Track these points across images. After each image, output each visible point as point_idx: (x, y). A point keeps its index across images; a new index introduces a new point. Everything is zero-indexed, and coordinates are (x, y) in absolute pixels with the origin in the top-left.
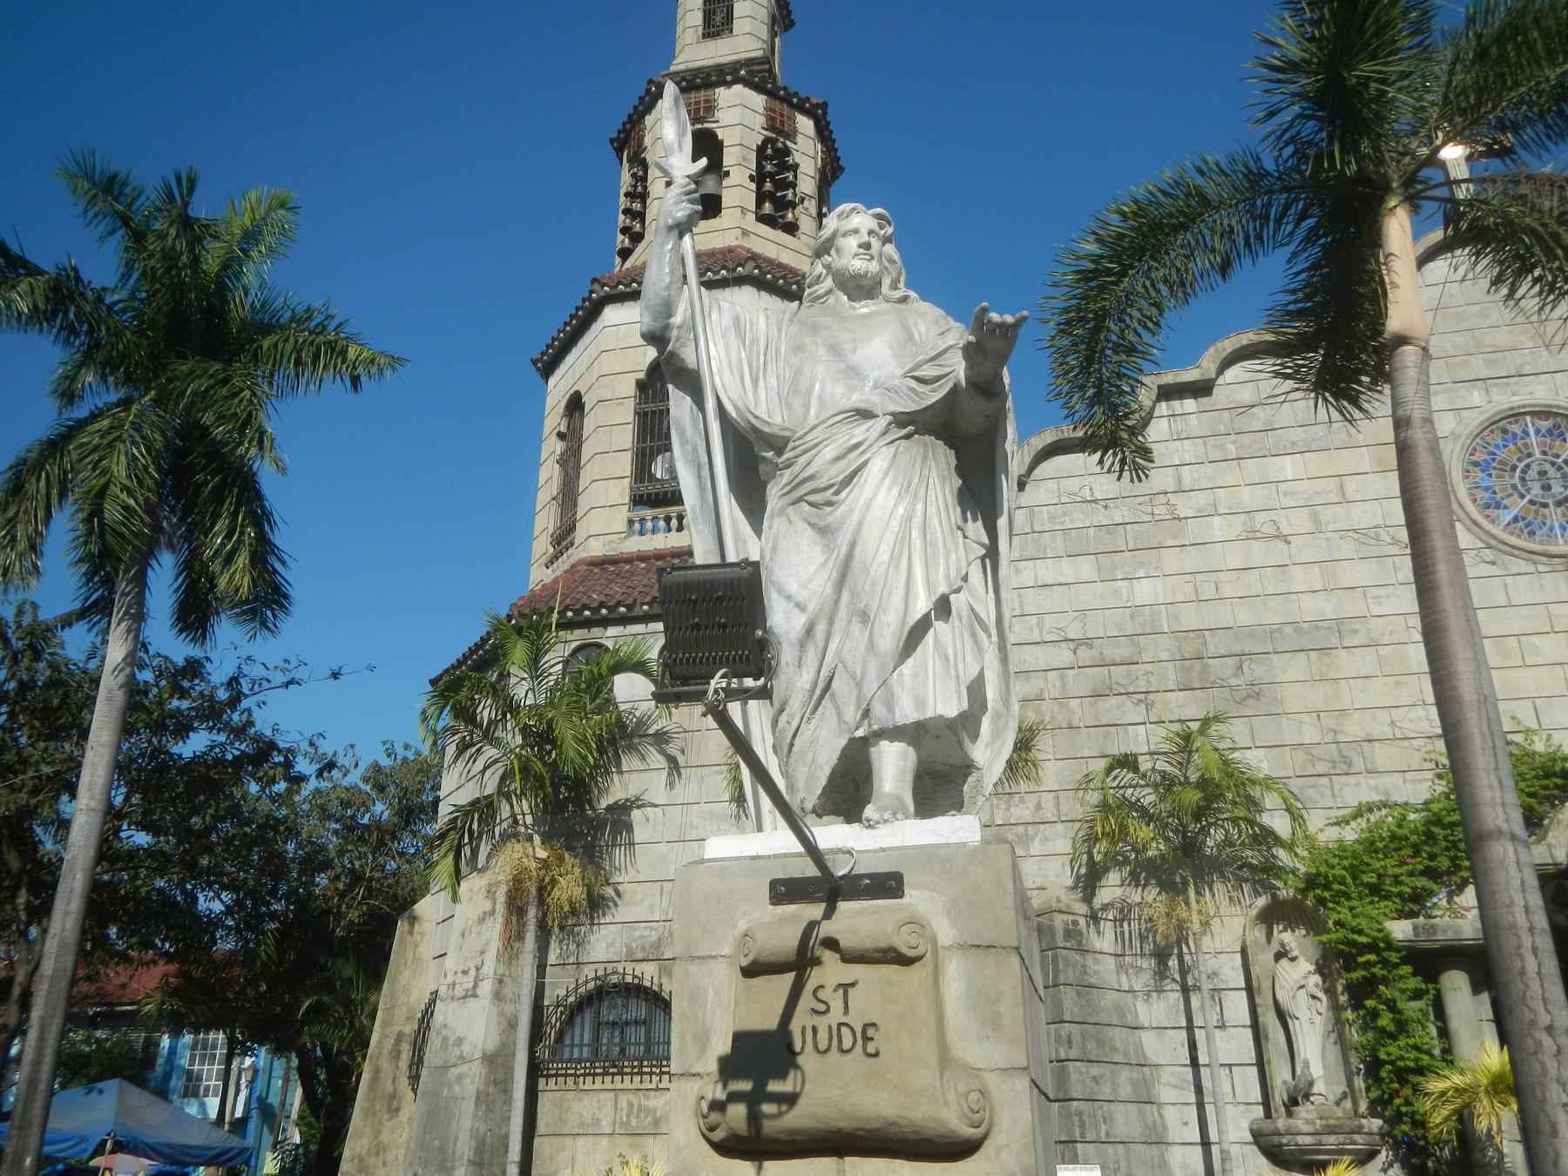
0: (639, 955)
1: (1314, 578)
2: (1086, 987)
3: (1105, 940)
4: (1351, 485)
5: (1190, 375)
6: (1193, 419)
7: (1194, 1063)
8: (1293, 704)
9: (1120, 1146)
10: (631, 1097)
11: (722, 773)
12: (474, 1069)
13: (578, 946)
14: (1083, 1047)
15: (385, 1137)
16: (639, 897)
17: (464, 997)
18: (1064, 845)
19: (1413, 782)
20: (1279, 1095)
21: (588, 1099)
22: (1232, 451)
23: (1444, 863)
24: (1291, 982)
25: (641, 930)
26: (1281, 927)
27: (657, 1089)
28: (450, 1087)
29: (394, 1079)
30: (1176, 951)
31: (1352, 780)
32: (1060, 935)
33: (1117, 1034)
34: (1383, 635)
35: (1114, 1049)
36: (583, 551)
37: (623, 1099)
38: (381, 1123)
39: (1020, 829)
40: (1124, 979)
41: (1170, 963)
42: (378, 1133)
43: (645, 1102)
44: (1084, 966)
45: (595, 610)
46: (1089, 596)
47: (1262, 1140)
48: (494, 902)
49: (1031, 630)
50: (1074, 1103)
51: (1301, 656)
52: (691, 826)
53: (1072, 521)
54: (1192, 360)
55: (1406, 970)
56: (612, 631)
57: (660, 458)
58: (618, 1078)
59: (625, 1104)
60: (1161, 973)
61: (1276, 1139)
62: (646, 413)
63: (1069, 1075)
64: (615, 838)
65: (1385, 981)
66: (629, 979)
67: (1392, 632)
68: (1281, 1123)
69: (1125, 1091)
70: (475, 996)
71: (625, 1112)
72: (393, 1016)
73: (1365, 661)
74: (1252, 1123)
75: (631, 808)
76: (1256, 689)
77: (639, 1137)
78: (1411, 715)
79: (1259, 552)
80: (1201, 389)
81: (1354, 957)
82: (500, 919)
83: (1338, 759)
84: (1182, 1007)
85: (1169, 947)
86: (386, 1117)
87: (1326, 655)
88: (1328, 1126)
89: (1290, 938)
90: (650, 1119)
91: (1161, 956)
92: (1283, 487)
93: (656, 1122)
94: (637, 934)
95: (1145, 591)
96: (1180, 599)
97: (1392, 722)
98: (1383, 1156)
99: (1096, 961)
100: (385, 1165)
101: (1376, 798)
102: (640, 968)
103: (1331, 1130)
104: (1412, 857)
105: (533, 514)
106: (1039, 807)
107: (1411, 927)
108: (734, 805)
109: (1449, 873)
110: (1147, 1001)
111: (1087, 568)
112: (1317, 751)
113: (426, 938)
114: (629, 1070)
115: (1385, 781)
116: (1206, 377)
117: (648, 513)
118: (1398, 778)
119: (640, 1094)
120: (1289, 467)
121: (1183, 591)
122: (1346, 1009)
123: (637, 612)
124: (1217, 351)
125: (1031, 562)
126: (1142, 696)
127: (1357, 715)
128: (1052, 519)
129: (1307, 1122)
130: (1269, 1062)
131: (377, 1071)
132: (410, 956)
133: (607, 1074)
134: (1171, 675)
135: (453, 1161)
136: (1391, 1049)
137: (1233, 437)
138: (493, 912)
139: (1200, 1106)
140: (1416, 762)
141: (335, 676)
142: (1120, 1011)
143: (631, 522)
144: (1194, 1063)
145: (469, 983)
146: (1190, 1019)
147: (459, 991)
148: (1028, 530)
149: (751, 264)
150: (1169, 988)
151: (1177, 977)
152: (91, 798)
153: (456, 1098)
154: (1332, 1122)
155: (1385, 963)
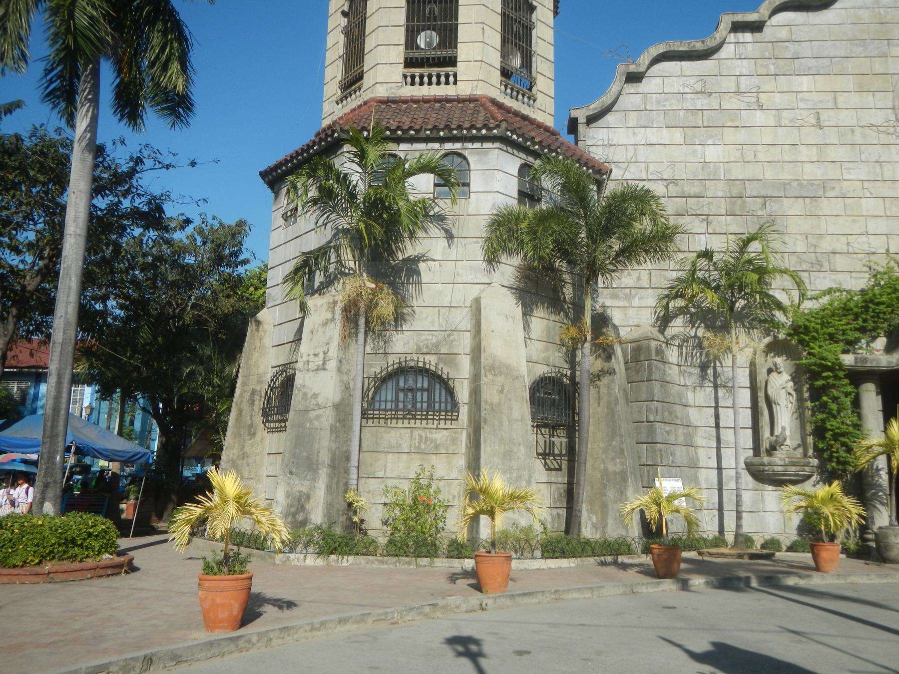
0: (425, 350)
1: (812, 153)
2: (665, 382)
3: (673, 355)
4: (841, 98)
5: (752, 17)
6: (750, 46)
7: (717, 426)
8: (792, 229)
9: (678, 468)
10: (421, 432)
12: (327, 412)
13: (385, 343)
14: (663, 415)
15: (247, 449)
16: (424, 315)
17: (317, 370)
18: (652, 301)
19: (856, 278)
20: (765, 445)
21: (393, 432)
22: (772, 69)
23: (870, 325)
24: (778, 385)
25: (425, 336)
26: (772, 355)
27: (437, 428)
28: (311, 422)
29: (251, 416)
30: (712, 365)
31: (821, 275)
32: (653, 352)
33: (678, 408)
34: (849, 192)
35: (676, 417)
36: (372, 93)
37: (416, 433)
38: (244, 441)
39: (627, 291)
40: (682, 378)
41: (709, 371)
42: (243, 447)
43: (428, 435)
44: (664, 371)
45: (393, 131)
46: (677, 153)
47: (752, 468)
48: (333, 313)
49: (641, 171)
50: (658, 445)
51: (801, 200)
52: (458, 274)
53: (670, 105)
54: (754, 8)
55: (846, 381)
56: (403, 146)
57: (423, 34)
58: (412, 421)
59: (417, 436)
60: (703, 376)
61: (761, 468)
63: (655, 430)
64: (408, 279)
65: (834, 386)
66: (421, 364)
67: (854, 190)
68: (766, 459)
69: (681, 439)
70: (324, 369)
71: (417, 440)
73: (837, 206)
74: (746, 459)
75: (418, 261)
76: (773, 218)
77: (427, 455)
78: (859, 240)
79: (782, 135)
80: (756, 27)
81: (819, 373)
82: (339, 324)
83: (815, 262)
84: (713, 396)
85: (709, 361)
86: (248, 438)
87: (815, 201)
88: (792, 462)
89: (779, 360)
90: (433, 445)
91: (703, 367)
92: (800, 95)
93: (437, 447)
94: (424, 337)
95: (712, 153)
96: (732, 160)
97: (848, 243)
98: (814, 478)
99: (670, 368)
100: (248, 465)
101: (834, 286)
102: (428, 358)
103: (794, 464)
104: (854, 320)
105: (324, 67)
106: (639, 278)
107: (853, 359)
108: (485, 264)
109: (870, 331)
110: (694, 391)
111: (677, 136)
112: (804, 257)
114: (419, 417)
115: (840, 277)
116: (762, 19)
117: (417, 71)
118: (847, 275)
119: (426, 430)
120: (805, 83)
121: (735, 155)
122: (807, 401)
123: (422, 135)
125: (644, 129)
126: (705, 217)
127: (828, 238)
128: (658, 102)
129: (781, 459)
130: (762, 427)
131: (240, 412)
132: (258, 344)
133: (406, 418)
134: (723, 206)
135: (317, 465)
136: (835, 424)
137: (773, 61)
138: (333, 319)
139: (718, 449)
140: (859, 266)
141: (193, 164)
142: (680, 396)
143: (405, 76)
144: (717, 426)
146: (717, 402)
147: (312, 366)
148: (642, 108)
150: (706, 385)
151: (712, 379)
153: (317, 429)
154: (794, 460)
155: (836, 377)
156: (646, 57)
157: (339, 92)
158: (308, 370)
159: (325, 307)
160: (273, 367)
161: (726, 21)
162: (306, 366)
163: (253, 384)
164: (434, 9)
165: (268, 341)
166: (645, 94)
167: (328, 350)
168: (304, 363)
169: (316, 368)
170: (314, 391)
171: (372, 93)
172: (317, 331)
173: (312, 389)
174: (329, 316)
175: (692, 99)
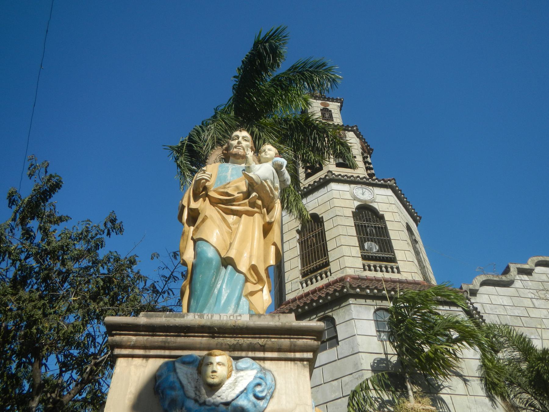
5: (526, 266)
11: (474, 381)
36: (343, 272)
53: (499, 311)
54: (526, 263)
80: (529, 272)
116: (532, 268)
117: (372, 263)
124: (532, 260)
143: (364, 266)
149: (393, 181)
156: (477, 281)
157: (300, 276)
161: (513, 268)
164: (372, 230)
166: (482, 304)
171: (343, 272)
175: (511, 309)
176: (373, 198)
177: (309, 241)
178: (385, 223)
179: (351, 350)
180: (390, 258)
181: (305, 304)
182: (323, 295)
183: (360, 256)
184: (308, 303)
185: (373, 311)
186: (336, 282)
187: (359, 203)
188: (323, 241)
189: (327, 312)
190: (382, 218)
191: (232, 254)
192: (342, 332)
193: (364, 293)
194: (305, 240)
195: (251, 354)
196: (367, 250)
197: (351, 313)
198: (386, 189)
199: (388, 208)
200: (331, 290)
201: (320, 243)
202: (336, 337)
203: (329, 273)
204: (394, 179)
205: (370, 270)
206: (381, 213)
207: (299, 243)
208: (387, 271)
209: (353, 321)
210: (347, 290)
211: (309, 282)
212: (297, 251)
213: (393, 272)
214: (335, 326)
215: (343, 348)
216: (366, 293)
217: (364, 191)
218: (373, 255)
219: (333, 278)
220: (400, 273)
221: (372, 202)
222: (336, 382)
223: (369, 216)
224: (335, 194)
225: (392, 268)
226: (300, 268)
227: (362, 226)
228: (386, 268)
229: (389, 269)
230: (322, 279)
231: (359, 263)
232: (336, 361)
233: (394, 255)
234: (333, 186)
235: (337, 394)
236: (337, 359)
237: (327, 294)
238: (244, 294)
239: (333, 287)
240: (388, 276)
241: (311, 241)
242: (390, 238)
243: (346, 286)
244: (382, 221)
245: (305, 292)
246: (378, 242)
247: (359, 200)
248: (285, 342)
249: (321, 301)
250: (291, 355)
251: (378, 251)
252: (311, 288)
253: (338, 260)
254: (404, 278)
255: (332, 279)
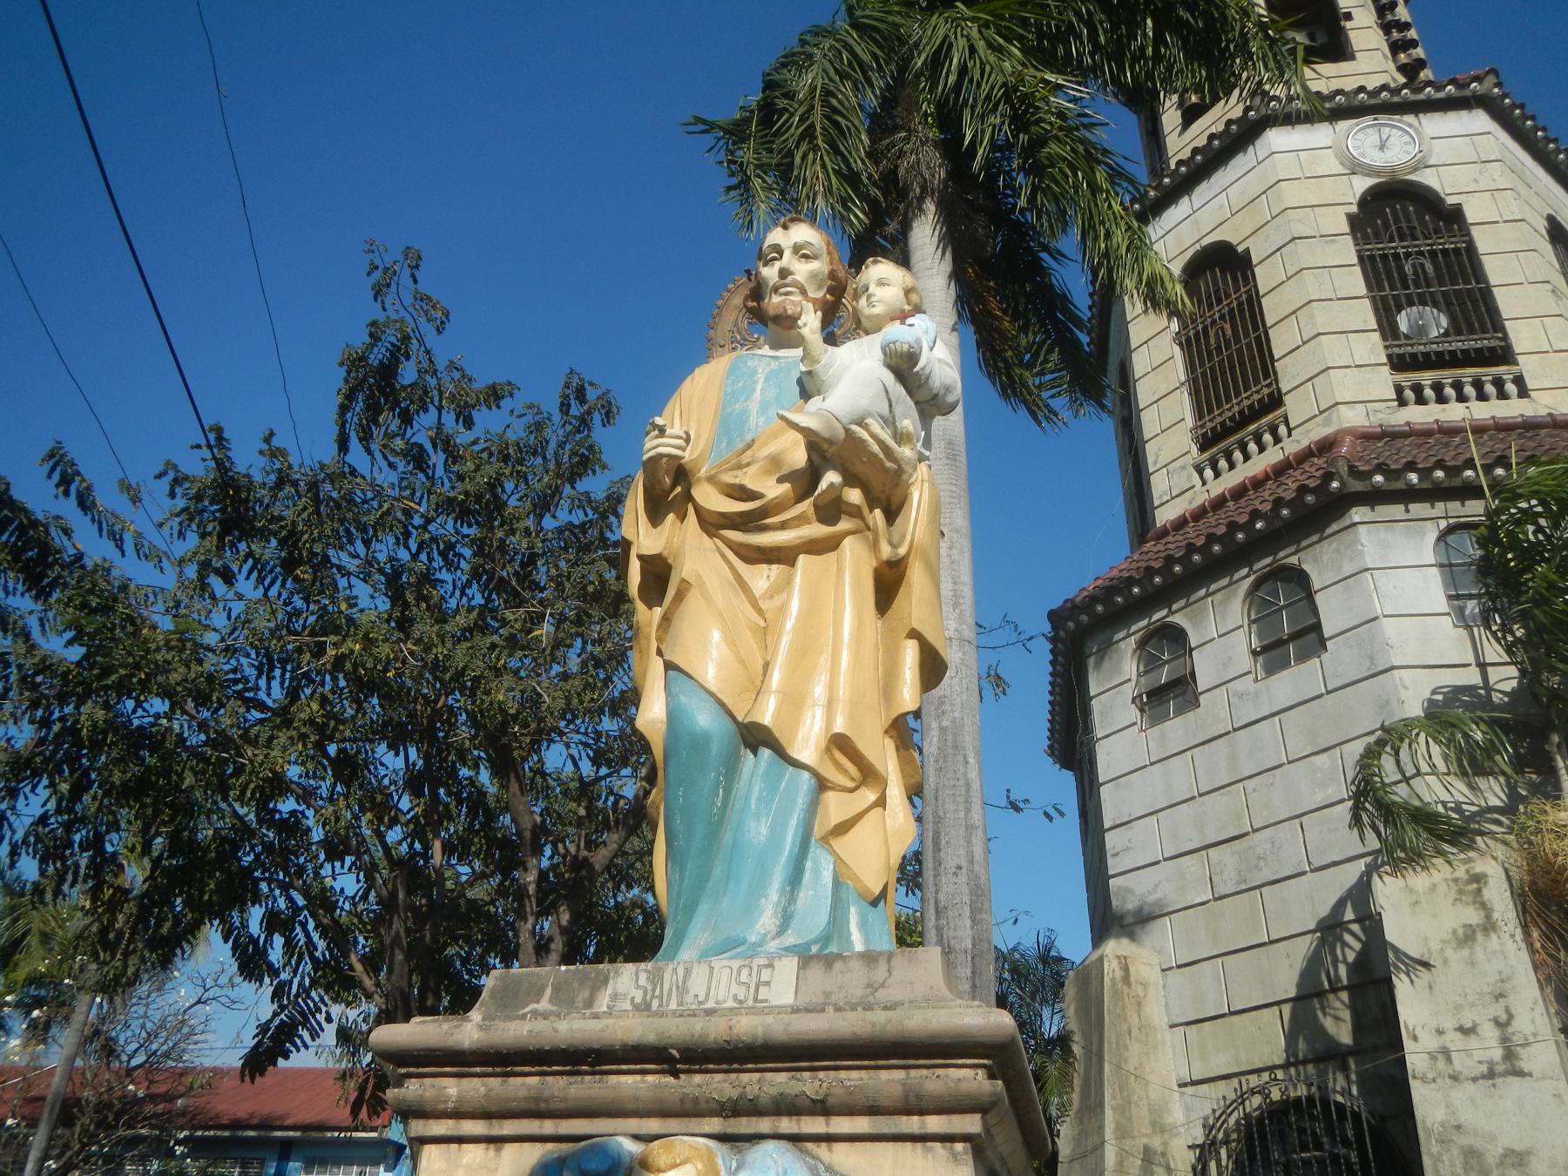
17: (1491, 1075)
36: (1327, 423)
48: (1484, 907)
62: (1372, 258)
70: (1520, 1073)
72: (1130, 1119)
113: (1152, 991)
117: (1426, 378)
138: (1489, 926)
143: (1399, 390)
145: (1488, 1047)
149: (1491, 79)
152: (961, 620)
157: (1194, 449)
158: (1455, 1078)
159: (1445, 894)
160: (1182, 1085)
162: (1441, 1064)
163: (1144, 1137)
164: (1422, 266)
165: (1156, 1013)
167: (1510, 1017)
168: (1432, 1056)
169: (1484, 1069)
170: (1505, 1142)
171: (1327, 423)
172: (1445, 961)
173: (1493, 1138)
174: (1473, 916)
176: (1419, 156)
177: (1212, 333)
178: (1468, 234)
179: (1368, 663)
180: (1492, 350)
181: (1211, 538)
182: (1267, 507)
183: (1385, 360)
184: (1219, 533)
185: (1432, 536)
186: (1306, 455)
187: (1370, 182)
188: (1256, 329)
189: (1282, 554)
190: (1454, 217)
191: (767, 714)
192: (1332, 611)
193: (1399, 485)
194: (1197, 334)
195: (786, 1125)
196: (1407, 337)
197: (1361, 553)
198: (1464, 113)
199: (1475, 180)
200: (1288, 488)
201: (1247, 335)
202: (1317, 627)
203: (1282, 430)
204: (1493, 71)
205: (1421, 400)
206: (1450, 200)
207: (1180, 345)
208: (1482, 397)
209: (1367, 575)
210: (1342, 483)
211: (1223, 464)
212: (1178, 370)
213: (1503, 395)
214: (1310, 596)
215: (1339, 659)
216: (1407, 484)
217: (1384, 137)
218: (1428, 349)
219: (1298, 442)
220: (1529, 397)
221: (1415, 169)
222: (1324, 756)
223: (1408, 221)
224: (1283, 166)
225: (1499, 383)
226: (1190, 422)
227: (1384, 257)
228: (1478, 384)
229: (1490, 389)
230: (1262, 449)
231: (1383, 382)
232: (1321, 696)
233: (1505, 337)
234: (1276, 138)
235: (1330, 791)
236: (1324, 691)
237: (1278, 503)
238: (818, 831)
239: (1297, 473)
240: (1482, 411)
241: (1217, 335)
242: (1487, 282)
243: (1338, 473)
244: (1456, 227)
245: (1214, 494)
246: (1444, 303)
247: (1369, 171)
248: (888, 1080)
249: (1259, 526)
250: (912, 1124)
251: (1446, 334)
252: (1231, 480)
253: (1310, 383)
254: (1543, 412)
255: (1293, 446)
